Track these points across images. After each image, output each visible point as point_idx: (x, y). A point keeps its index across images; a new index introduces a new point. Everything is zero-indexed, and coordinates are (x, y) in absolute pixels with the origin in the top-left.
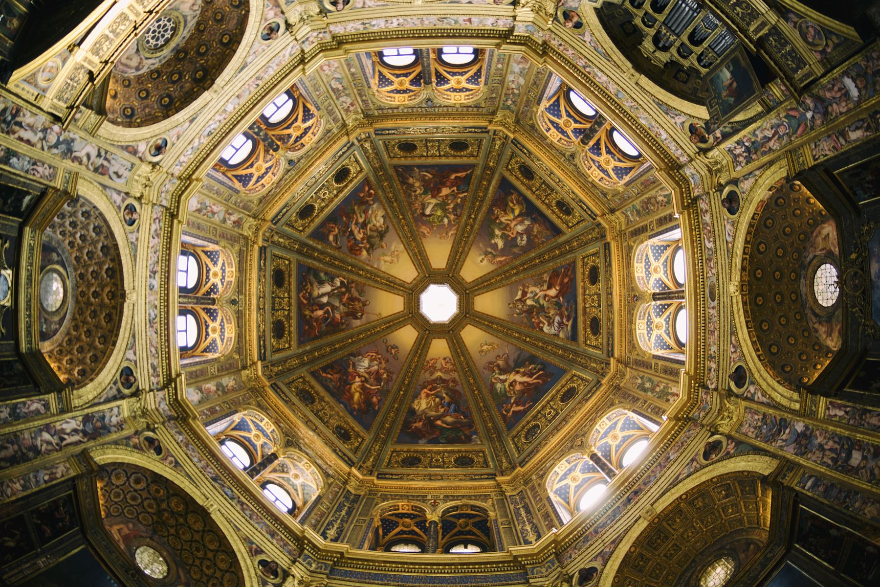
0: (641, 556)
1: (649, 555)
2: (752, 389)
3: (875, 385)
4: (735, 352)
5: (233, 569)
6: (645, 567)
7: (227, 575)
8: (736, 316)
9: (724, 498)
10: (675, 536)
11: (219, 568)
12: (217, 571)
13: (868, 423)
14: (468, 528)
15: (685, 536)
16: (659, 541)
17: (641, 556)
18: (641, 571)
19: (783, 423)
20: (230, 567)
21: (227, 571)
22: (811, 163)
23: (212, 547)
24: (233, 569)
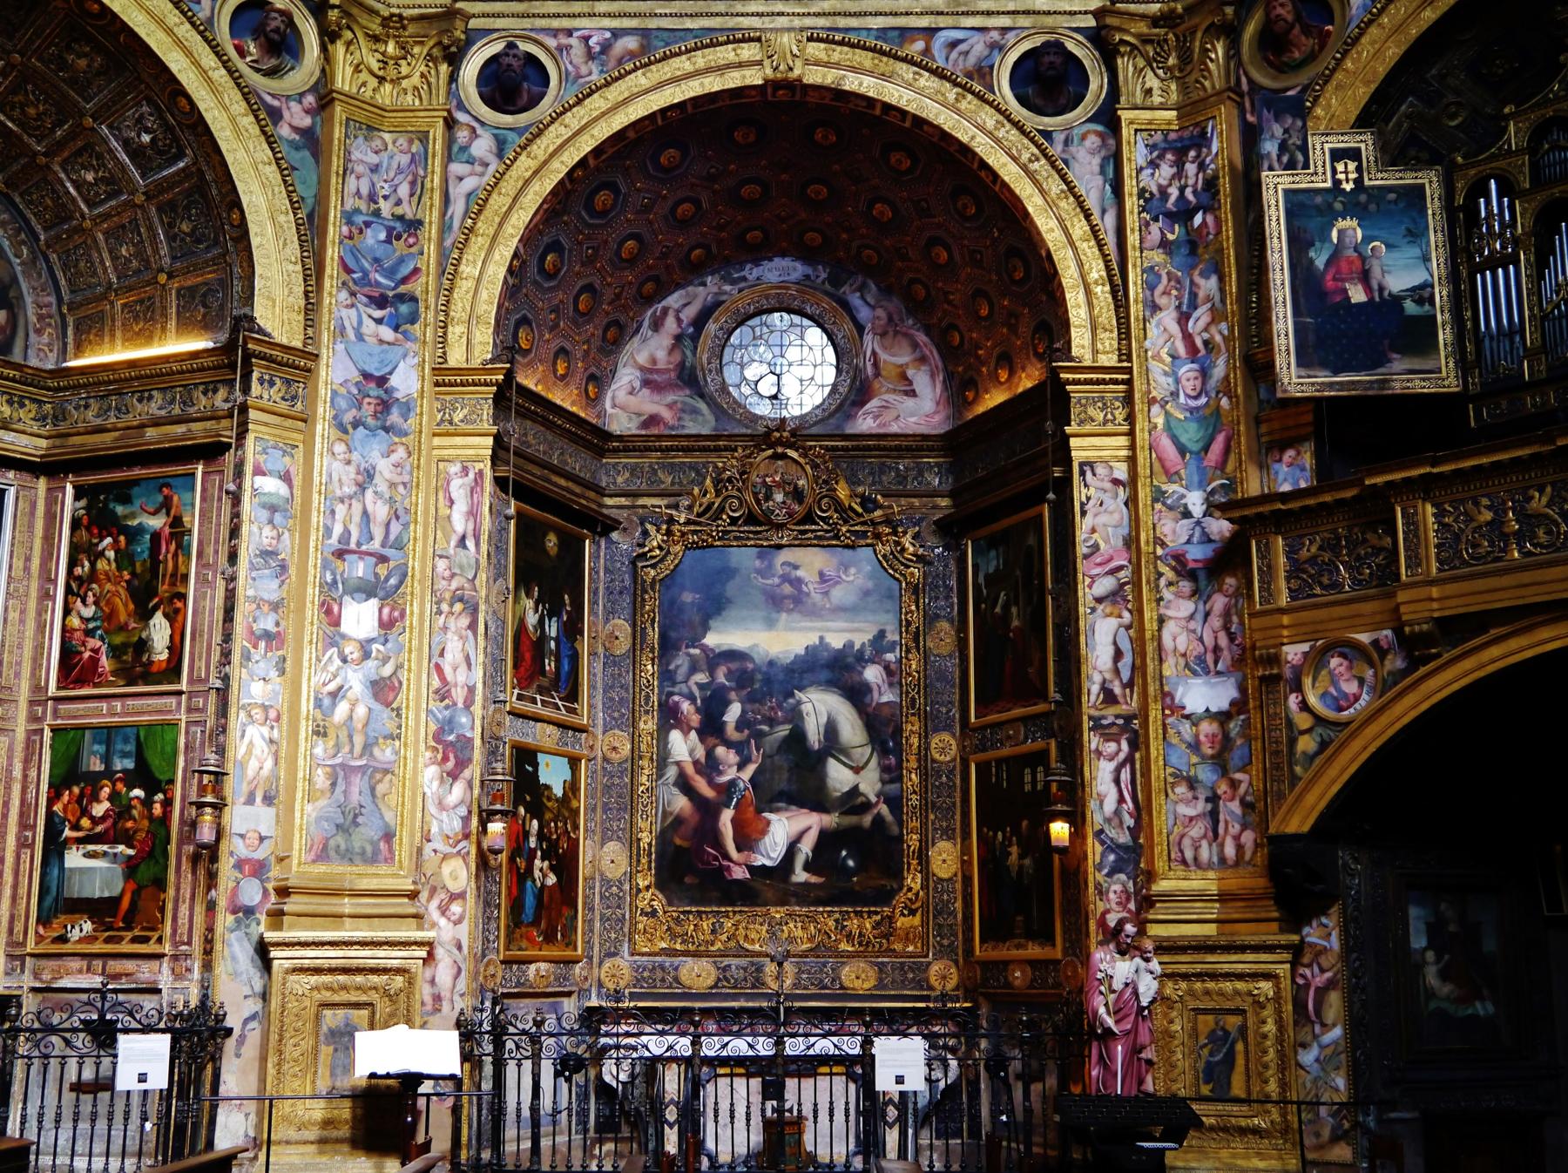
2: (483, 146)
3: (529, 604)
4: (590, 56)
8: (701, 59)
9: (126, 144)
13: (445, 629)
19: (404, 309)
22: (1081, 448)
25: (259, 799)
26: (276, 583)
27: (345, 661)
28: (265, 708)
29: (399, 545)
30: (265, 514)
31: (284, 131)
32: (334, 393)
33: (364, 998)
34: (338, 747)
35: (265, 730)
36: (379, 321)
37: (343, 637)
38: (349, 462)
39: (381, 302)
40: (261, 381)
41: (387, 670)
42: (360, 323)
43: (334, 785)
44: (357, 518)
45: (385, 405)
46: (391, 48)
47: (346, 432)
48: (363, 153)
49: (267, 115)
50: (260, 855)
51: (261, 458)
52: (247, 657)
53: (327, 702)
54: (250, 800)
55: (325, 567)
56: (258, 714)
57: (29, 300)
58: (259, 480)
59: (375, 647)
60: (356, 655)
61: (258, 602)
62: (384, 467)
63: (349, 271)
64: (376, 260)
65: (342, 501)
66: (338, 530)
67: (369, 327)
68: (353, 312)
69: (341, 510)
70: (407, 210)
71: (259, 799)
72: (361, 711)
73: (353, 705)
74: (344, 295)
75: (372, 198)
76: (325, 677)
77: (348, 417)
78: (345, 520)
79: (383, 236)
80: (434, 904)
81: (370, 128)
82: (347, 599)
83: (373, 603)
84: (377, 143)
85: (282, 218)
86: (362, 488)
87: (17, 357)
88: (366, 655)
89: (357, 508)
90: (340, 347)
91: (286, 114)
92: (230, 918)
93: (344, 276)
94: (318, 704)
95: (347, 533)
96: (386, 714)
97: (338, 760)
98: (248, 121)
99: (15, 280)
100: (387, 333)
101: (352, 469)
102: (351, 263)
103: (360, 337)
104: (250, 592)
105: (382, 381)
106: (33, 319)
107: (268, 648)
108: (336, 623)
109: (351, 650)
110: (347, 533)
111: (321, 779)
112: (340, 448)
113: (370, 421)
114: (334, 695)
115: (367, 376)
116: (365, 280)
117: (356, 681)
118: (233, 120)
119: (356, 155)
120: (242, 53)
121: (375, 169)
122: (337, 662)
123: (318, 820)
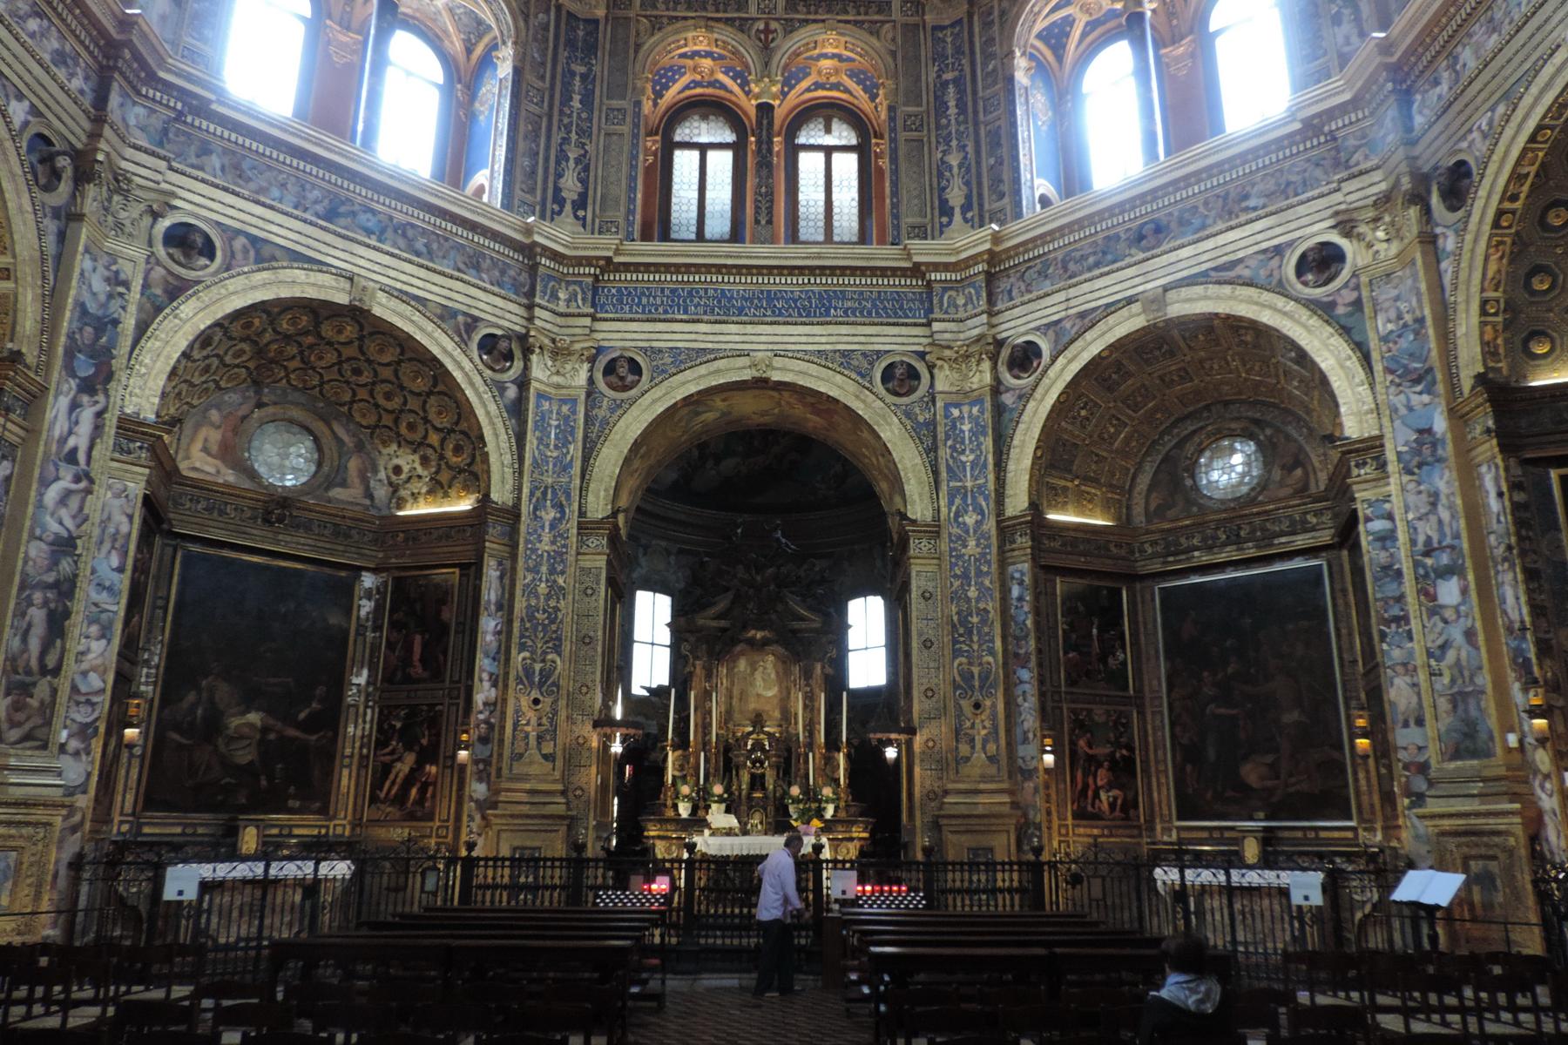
0: (1119, 365)
1: (1132, 368)
5: (440, 388)
6: (1119, 384)
7: (433, 400)
10: (1188, 358)
11: (411, 392)
12: (431, 432)
14: (833, 80)
15: (1207, 366)
16: (1157, 353)
17: (1119, 365)
18: (1110, 389)
20: (435, 385)
21: (430, 393)
23: (386, 359)
24: (440, 388)
25: (1412, 723)
26: (1395, 585)
27: (1446, 622)
28: (1405, 665)
29: (1457, 536)
30: (1378, 544)
31: (1341, 310)
32: (1399, 454)
33: (1491, 853)
34: (1453, 681)
35: (1408, 679)
36: (1420, 393)
37: (1442, 607)
38: (1420, 492)
39: (1417, 381)
40: (1357, 466)
41: (1469, 624)
42: (1408, 400)
43: (1455, 707)
44: (1435, 526)
45: (1434, 445)
46: (1387, 218)
47: (1412, 473)
48: (1386, 293)
49: (1324, 310)
50: (1422, 759)
51: (1368, 512)
52: (1383, 636)
53: (1438, 653)
54: (1406, 725)
55: (1416, 564)
56: (1400, 669)
57: (1312, 456)
58: (1370, 525)
59: (1462, 608)
60: (1454, 617)
61: (1385, 600)
62: (1441, 485)
63: (1392, 372)
64: (1411, 355)
65: (1420, 519)
66: (1421, 539)
67: (1415, 399)
68: (1402, 397)
69: (1420, 525)
70: (1418, 314)
71: (1412, 723)
72: (1464, 654)
73: (1459, 649)
74: (1392, 389)
75: (1400, 317)
76: (1431, 637)
77: (1414, 462)
78: (1427, 529)
79: (1411, 337)
80: (1537, 783)
81: (1388, 275)
82: (1439, 581)
83: (1455, 579)
84: (1396, 281)
85: (1348, 363)
86: (1434, 505)
87: (1313, 489)
88: (1459, 616)
89: (1433, 519)
90: (1398, 423)
91: (1339, 301)
92: (1406, 801)
93: (1390, 378)
94: (1430, 654)
95: (1429, 539)
96: (1474, 652)
97: (1455, 689)
98: (1314, 322)
99: (1301, 449)
100: (1426, 398)
101: (1424, 497)
102: (1393, 366)
103: (1410, 409)
104: (1379, 596)
105: (1429, 431)
106: (1317, 464)
107: (1399, 626)
108: (1434, 598)
109: (1449, 614)
110: (1429, 539)
111: (1444, 704)
112: (1411, 486)
113: (1430, 459)
114: (1444, 647)
115: (1421, 432)
116: (1407, 371)
117: (1456, 633)
118: (1305, 326)
119: (1382, 298)
120: (1305, 284)
121: (1397, 299)
122: (1441, 625)
123: (1448, 731)
